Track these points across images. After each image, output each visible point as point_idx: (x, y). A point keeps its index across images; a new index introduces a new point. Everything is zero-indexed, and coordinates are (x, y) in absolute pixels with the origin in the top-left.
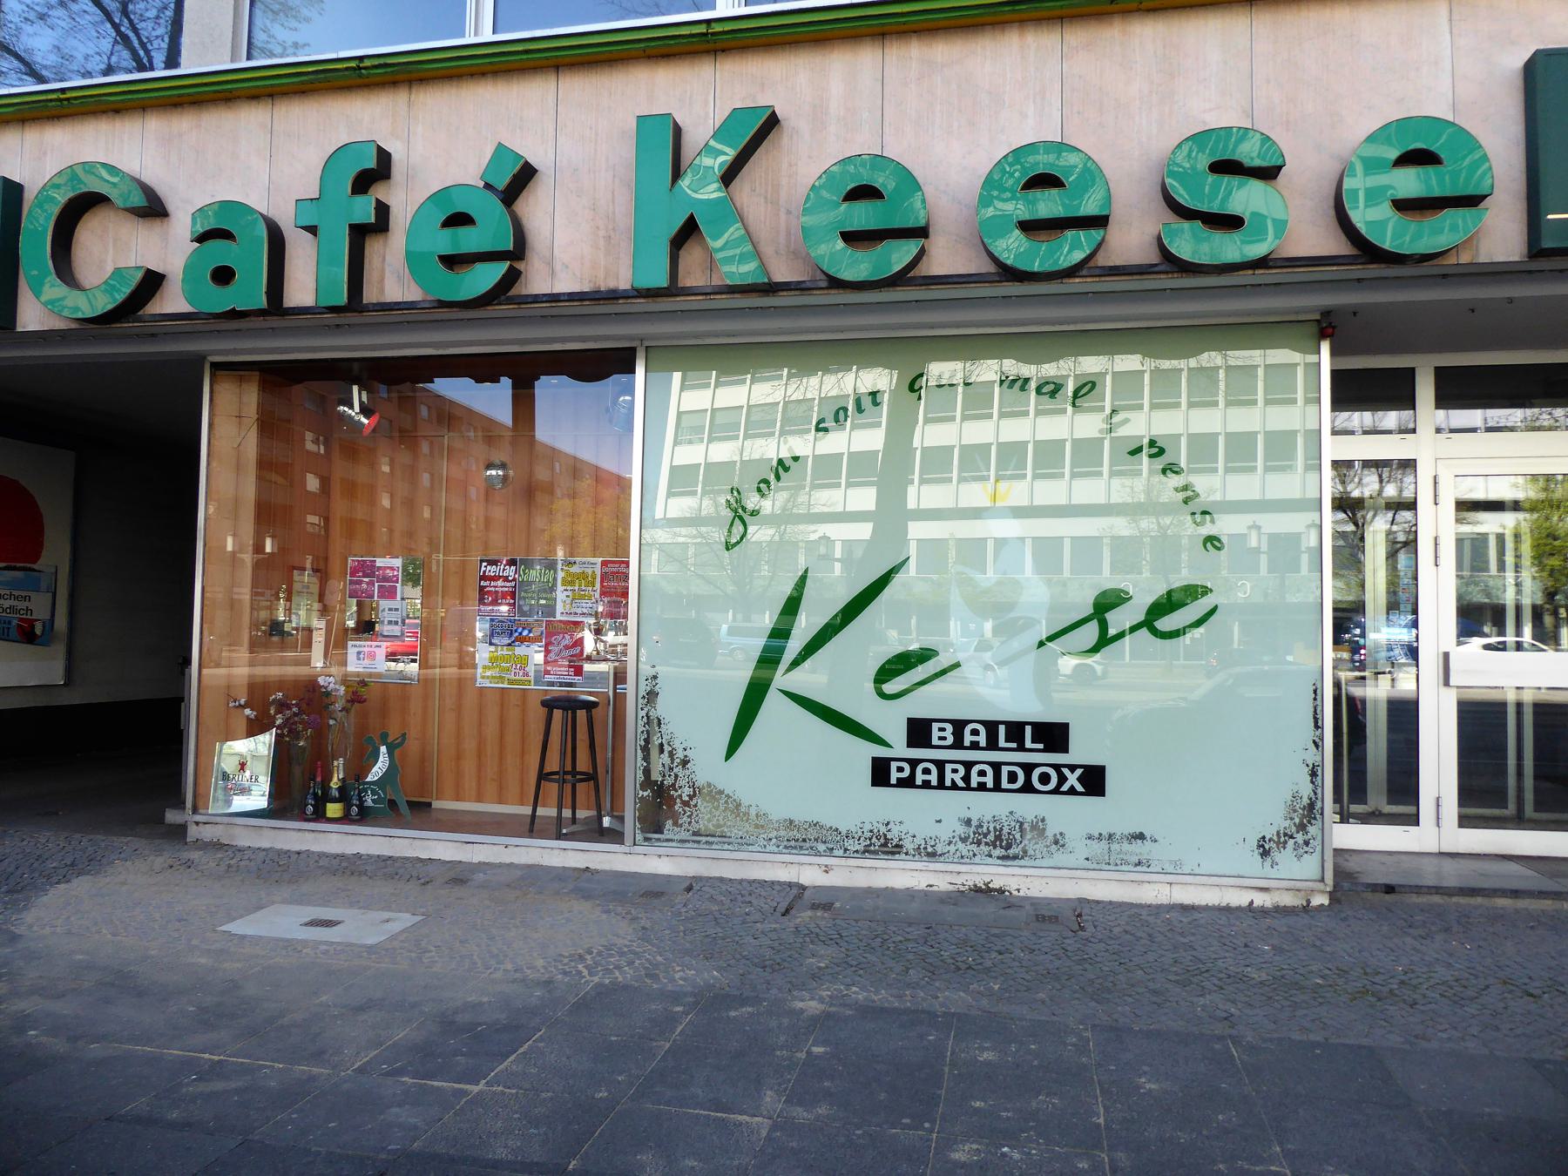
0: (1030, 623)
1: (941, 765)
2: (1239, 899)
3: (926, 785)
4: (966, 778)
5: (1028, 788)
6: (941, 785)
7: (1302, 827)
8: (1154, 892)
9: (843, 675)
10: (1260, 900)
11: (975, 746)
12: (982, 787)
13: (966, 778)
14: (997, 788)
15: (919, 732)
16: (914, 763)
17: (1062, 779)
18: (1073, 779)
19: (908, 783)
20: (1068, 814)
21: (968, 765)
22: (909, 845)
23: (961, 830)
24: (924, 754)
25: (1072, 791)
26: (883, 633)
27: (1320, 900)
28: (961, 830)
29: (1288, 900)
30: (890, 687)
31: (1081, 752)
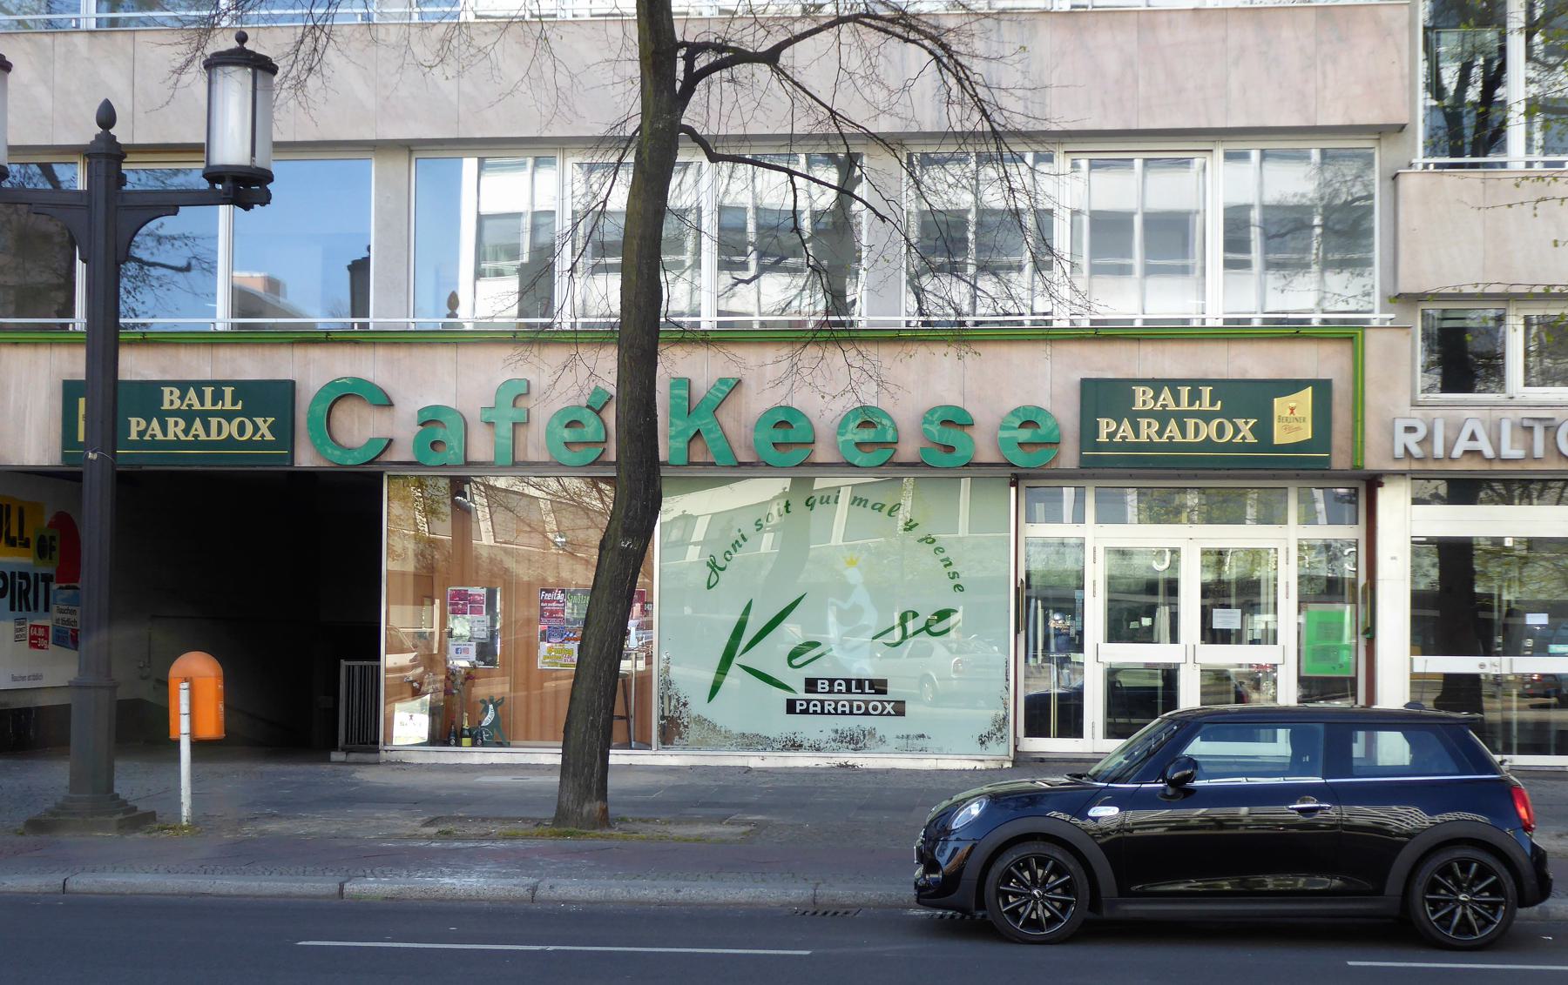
0: (867, 628)
1: (822, 702)
2: (969, 765)
3: (815, 712)
4: (836, 709)
5: (867, 713)
6: (822, 713)
7: (1000, 730)
8: (928, 763)
9: (770, 655)
10: (980, 766)
11: (840, 692)
12: (843, 713)
13: (836, 709)
14: (851, 713)
15: (811, 685)
16: (808, 701)
17: (884, 708)
18: (889, 708)
19: (806, 712)
20: (887, 726)
21: (836, 703)
22: (806, 744)
23: (833, 735)
24: (814, 696)
25: (889, 714)
26: (792, 632)
27: (1008, 765)
28: (833, 735)
29: (992, 765)
30: (796, 662)
31: (893, 692)
